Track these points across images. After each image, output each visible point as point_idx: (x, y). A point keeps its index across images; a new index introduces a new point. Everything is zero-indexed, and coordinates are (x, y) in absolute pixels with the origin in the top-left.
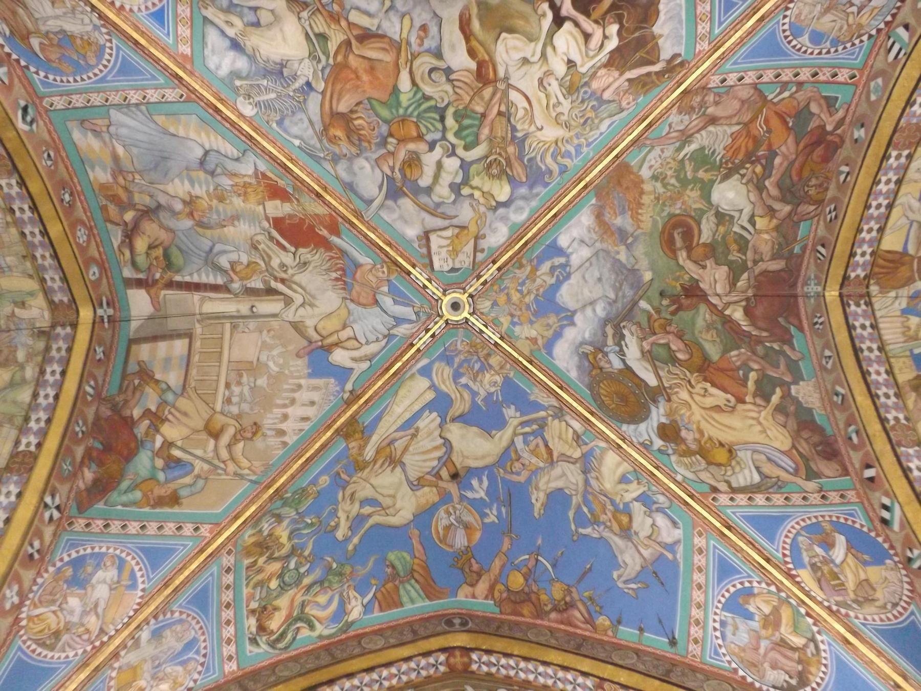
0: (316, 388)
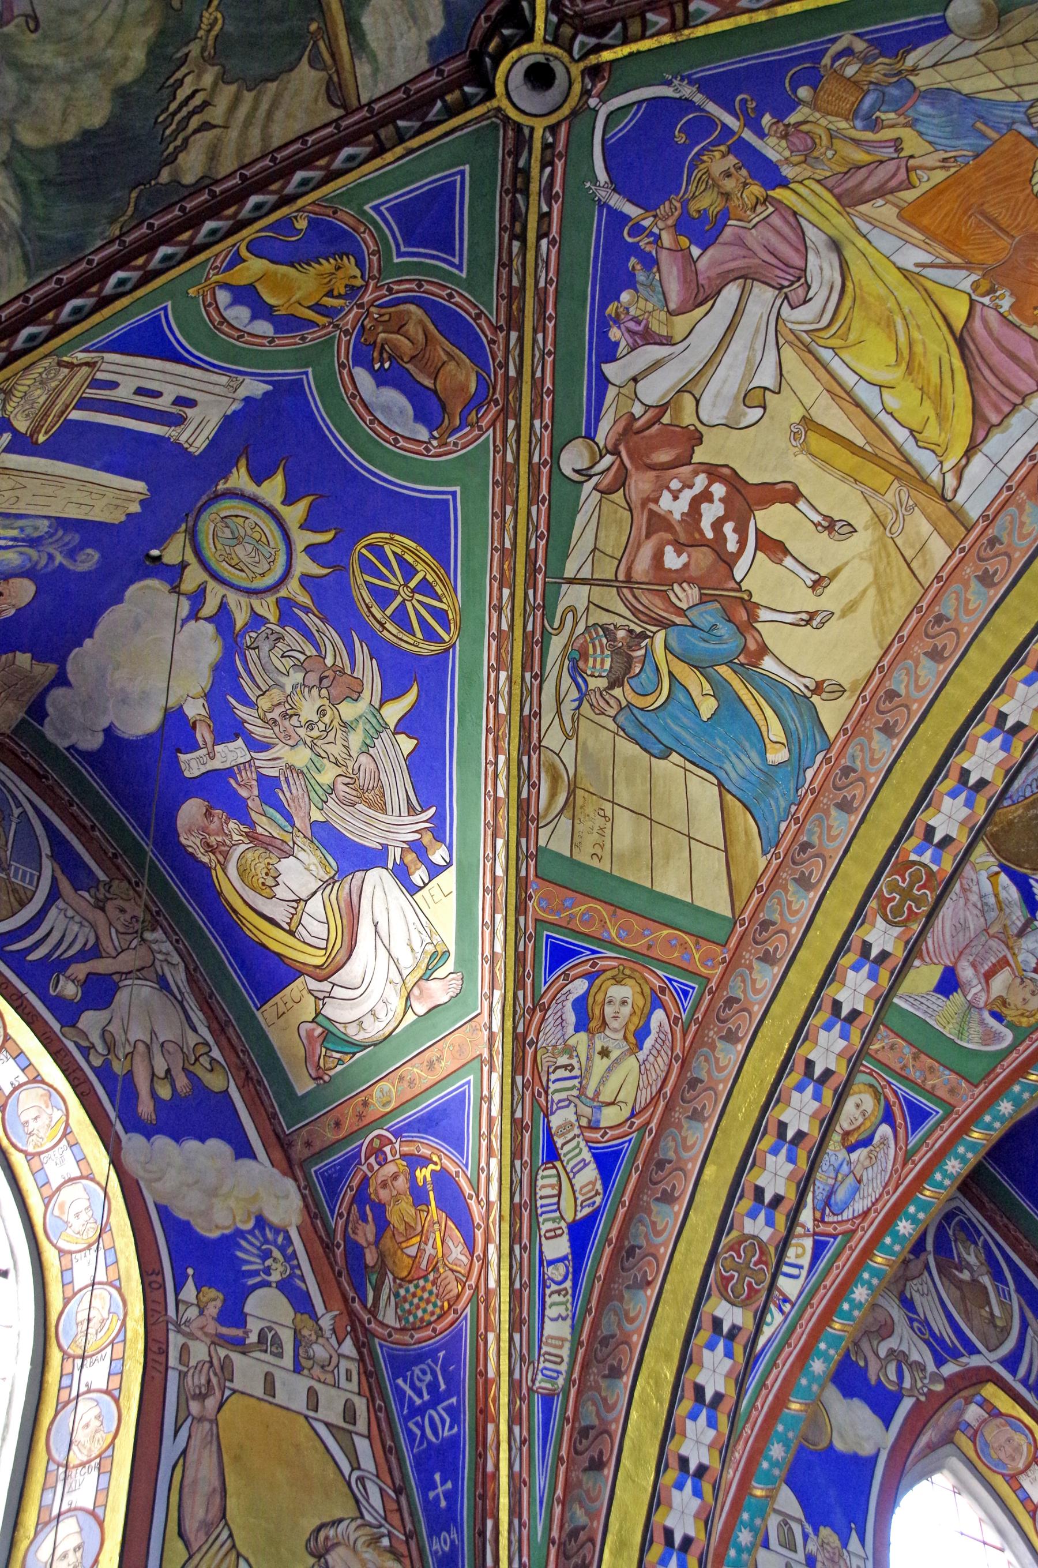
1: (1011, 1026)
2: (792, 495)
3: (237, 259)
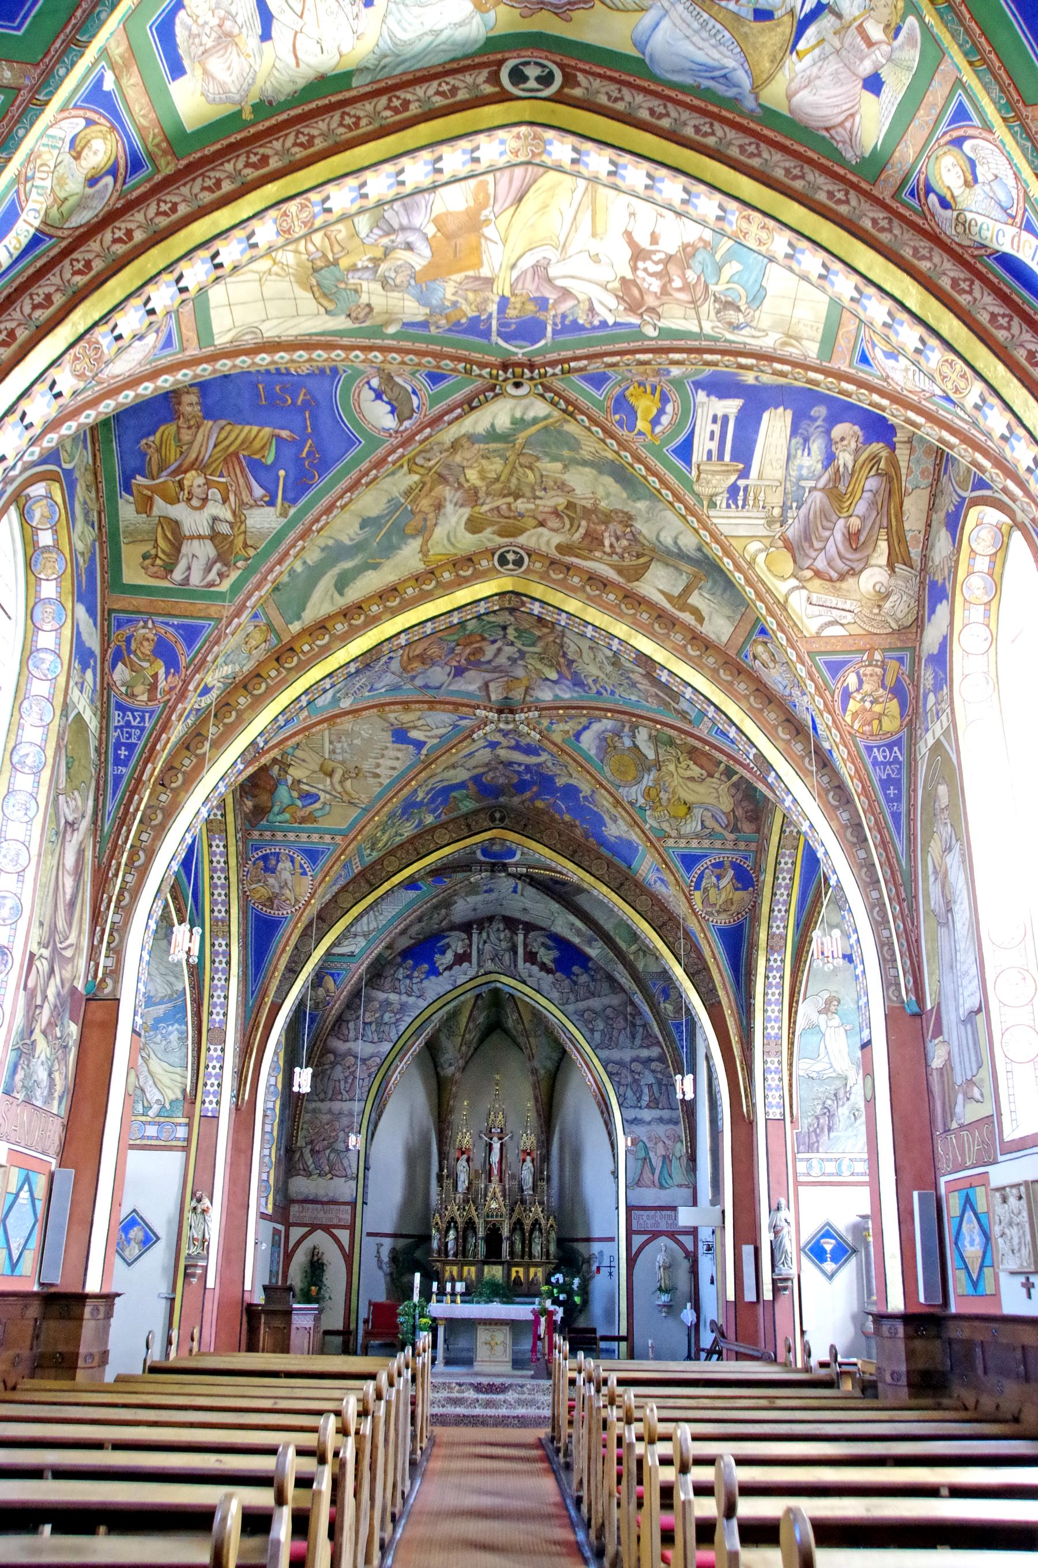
0: (399, 750)
1: (903, 19)
2: (628, 235)
3: (640, 433)
